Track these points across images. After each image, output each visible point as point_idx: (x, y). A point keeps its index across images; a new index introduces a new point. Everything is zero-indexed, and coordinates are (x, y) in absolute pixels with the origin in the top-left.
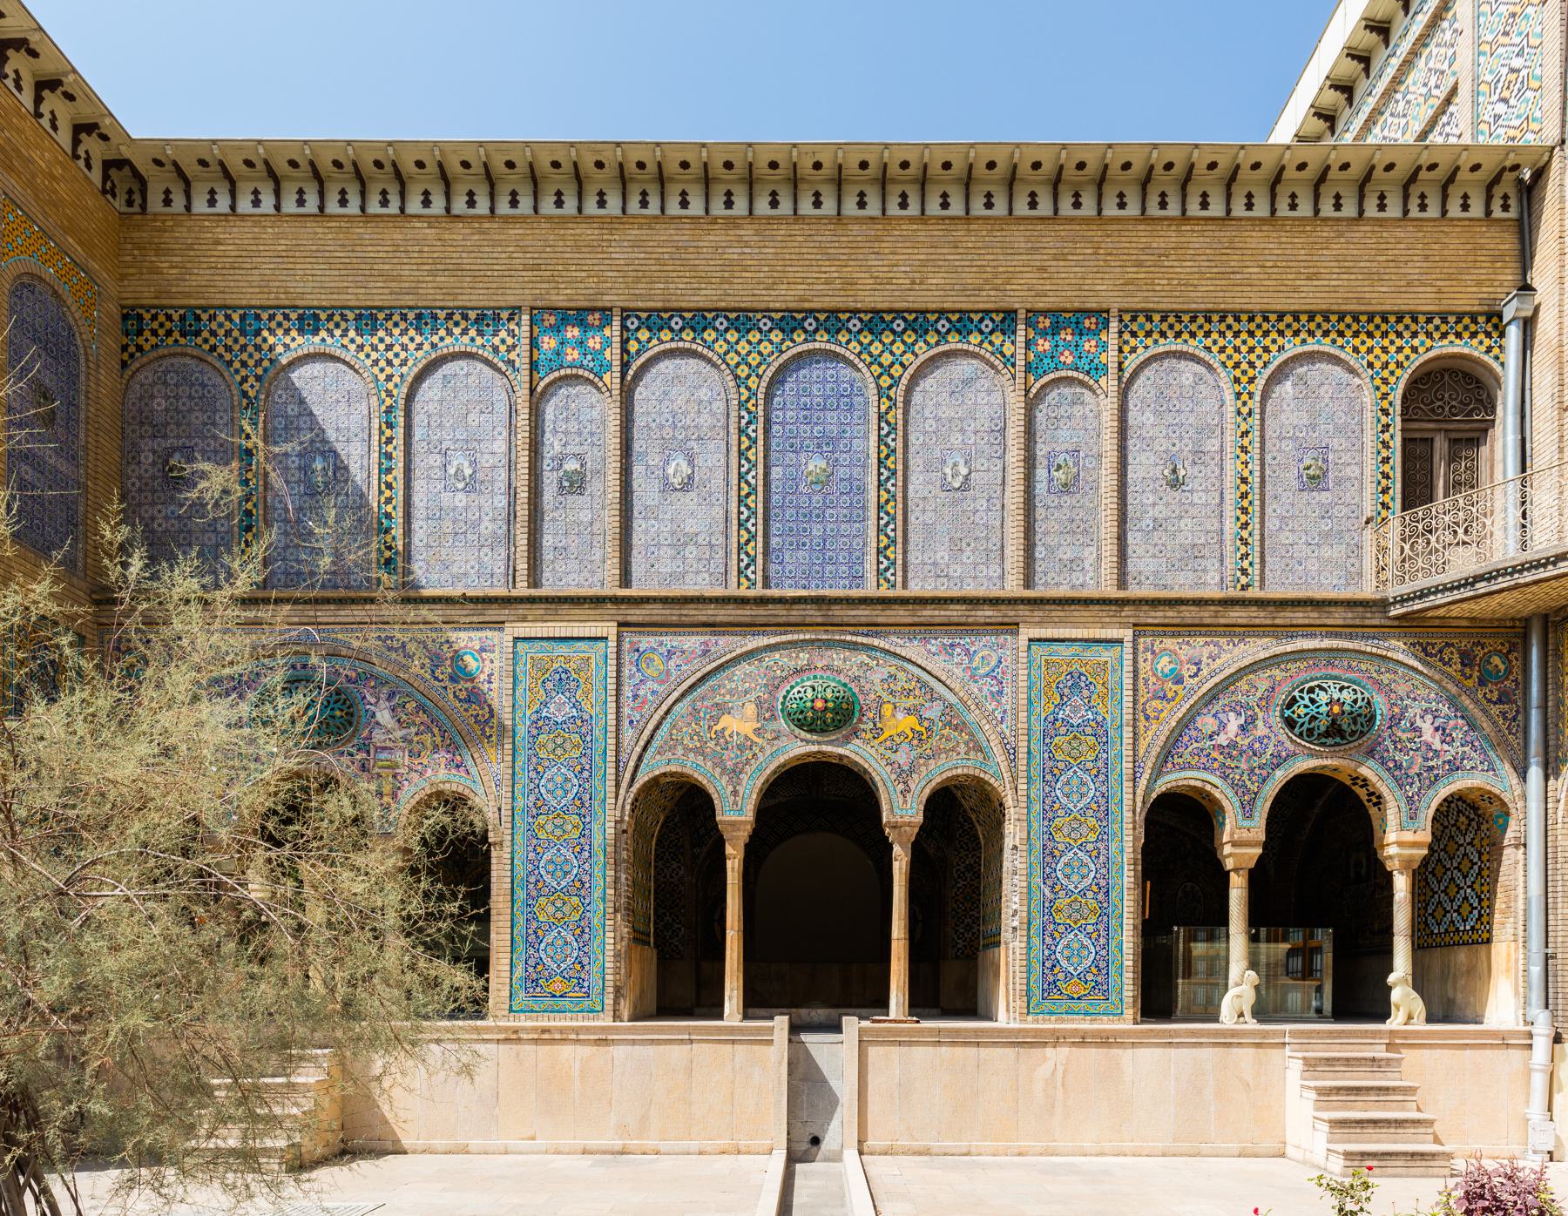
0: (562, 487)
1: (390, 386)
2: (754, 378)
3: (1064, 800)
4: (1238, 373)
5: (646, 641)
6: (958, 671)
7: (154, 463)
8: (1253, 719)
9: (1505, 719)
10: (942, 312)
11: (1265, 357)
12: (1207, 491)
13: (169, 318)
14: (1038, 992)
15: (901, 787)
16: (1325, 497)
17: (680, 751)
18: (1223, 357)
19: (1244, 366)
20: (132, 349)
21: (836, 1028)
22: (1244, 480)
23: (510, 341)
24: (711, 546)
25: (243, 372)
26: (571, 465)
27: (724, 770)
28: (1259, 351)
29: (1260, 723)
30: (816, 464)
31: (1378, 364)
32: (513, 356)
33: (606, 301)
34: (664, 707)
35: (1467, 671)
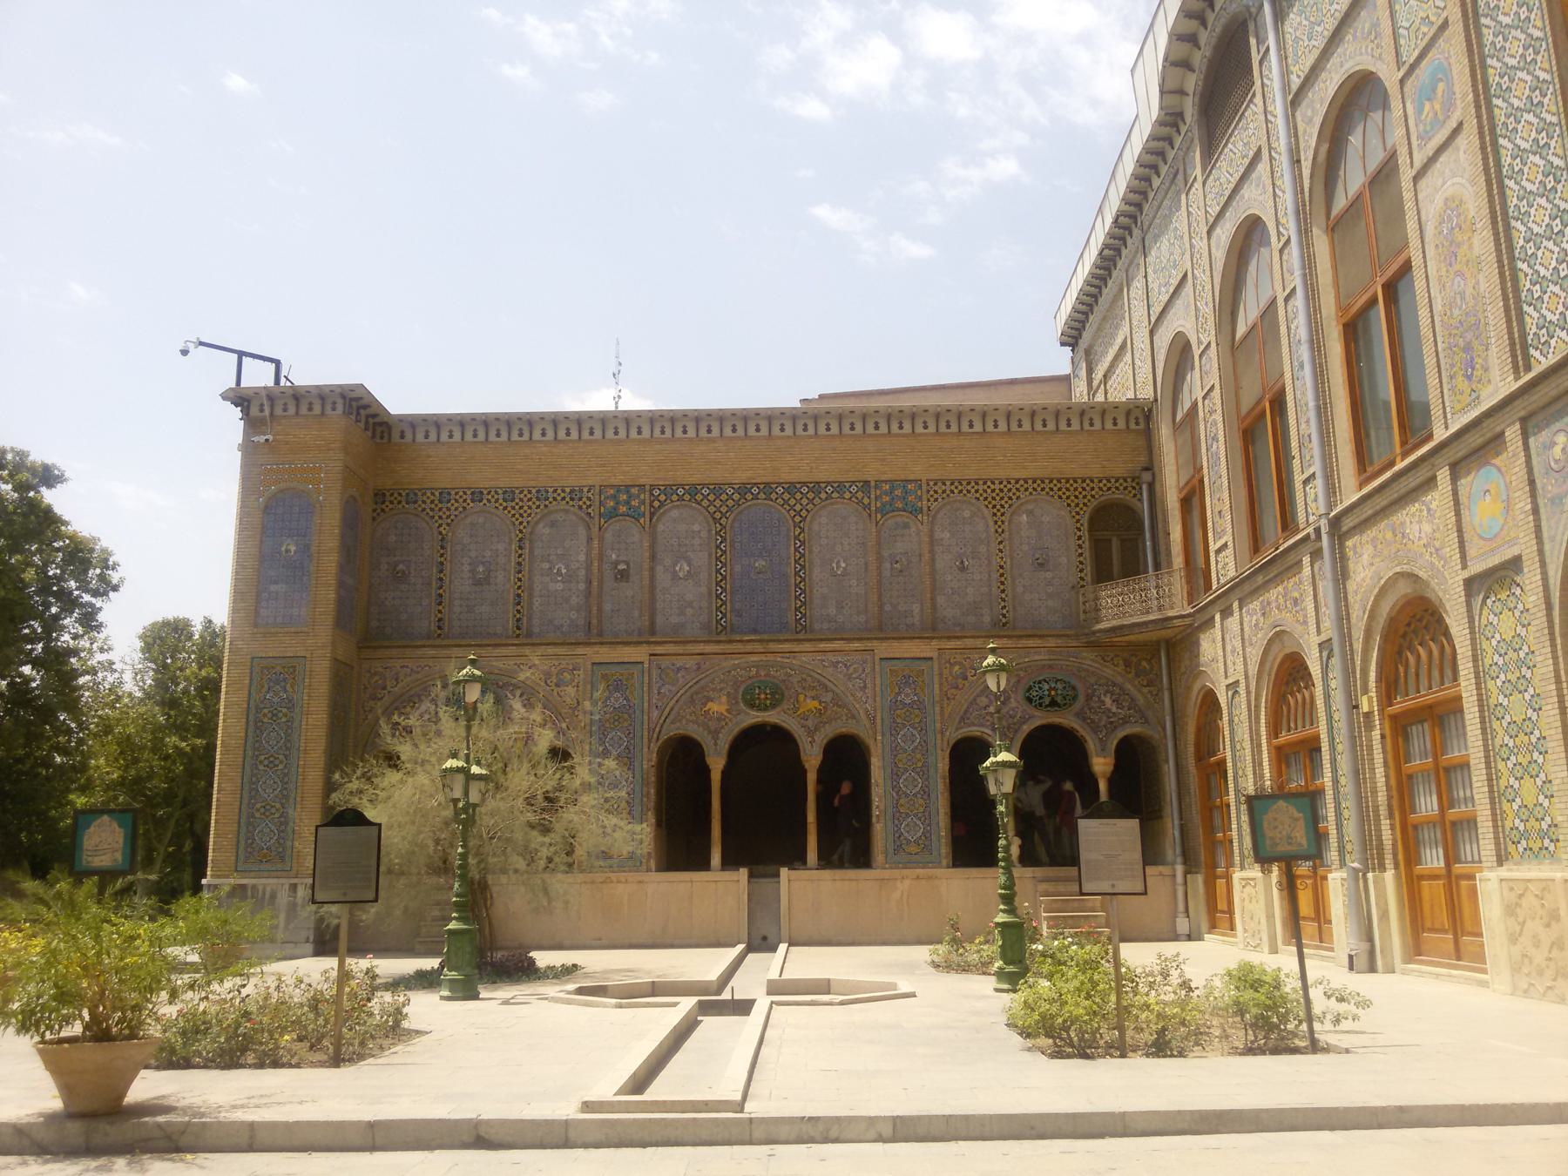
0: (616, 578)
1: (521, 527)
2: (724, 519)
3: (902, 744)
4: (995, 510)
5: (665, 662)
6: (841, 676)
7: (387, 570)
8: (1009, 698)
9: (1152, 695)
10: (828, 483)
11: (1010, 502)
12: (981, 573)
13: (400, 494)
14: (891, 851)
15: (810, 739)
16: (1049, 575)
17: (684, 722)
18: (986, 503)
19: (998, 507)
20: (379, 511)
21: (777, 875)
22: (1002, 567)
23: (588, 503)
24: (701, 608)
25: (440, 521)
26: (622, 567)
27: (710, 732)
28: (1006, 499)
29: (1012, 700)
30: (760, 563)
31: (1073, 505)
32: (590, 510)
33: (642, 481)
34: (675, 699)
35: (1128, 669)
